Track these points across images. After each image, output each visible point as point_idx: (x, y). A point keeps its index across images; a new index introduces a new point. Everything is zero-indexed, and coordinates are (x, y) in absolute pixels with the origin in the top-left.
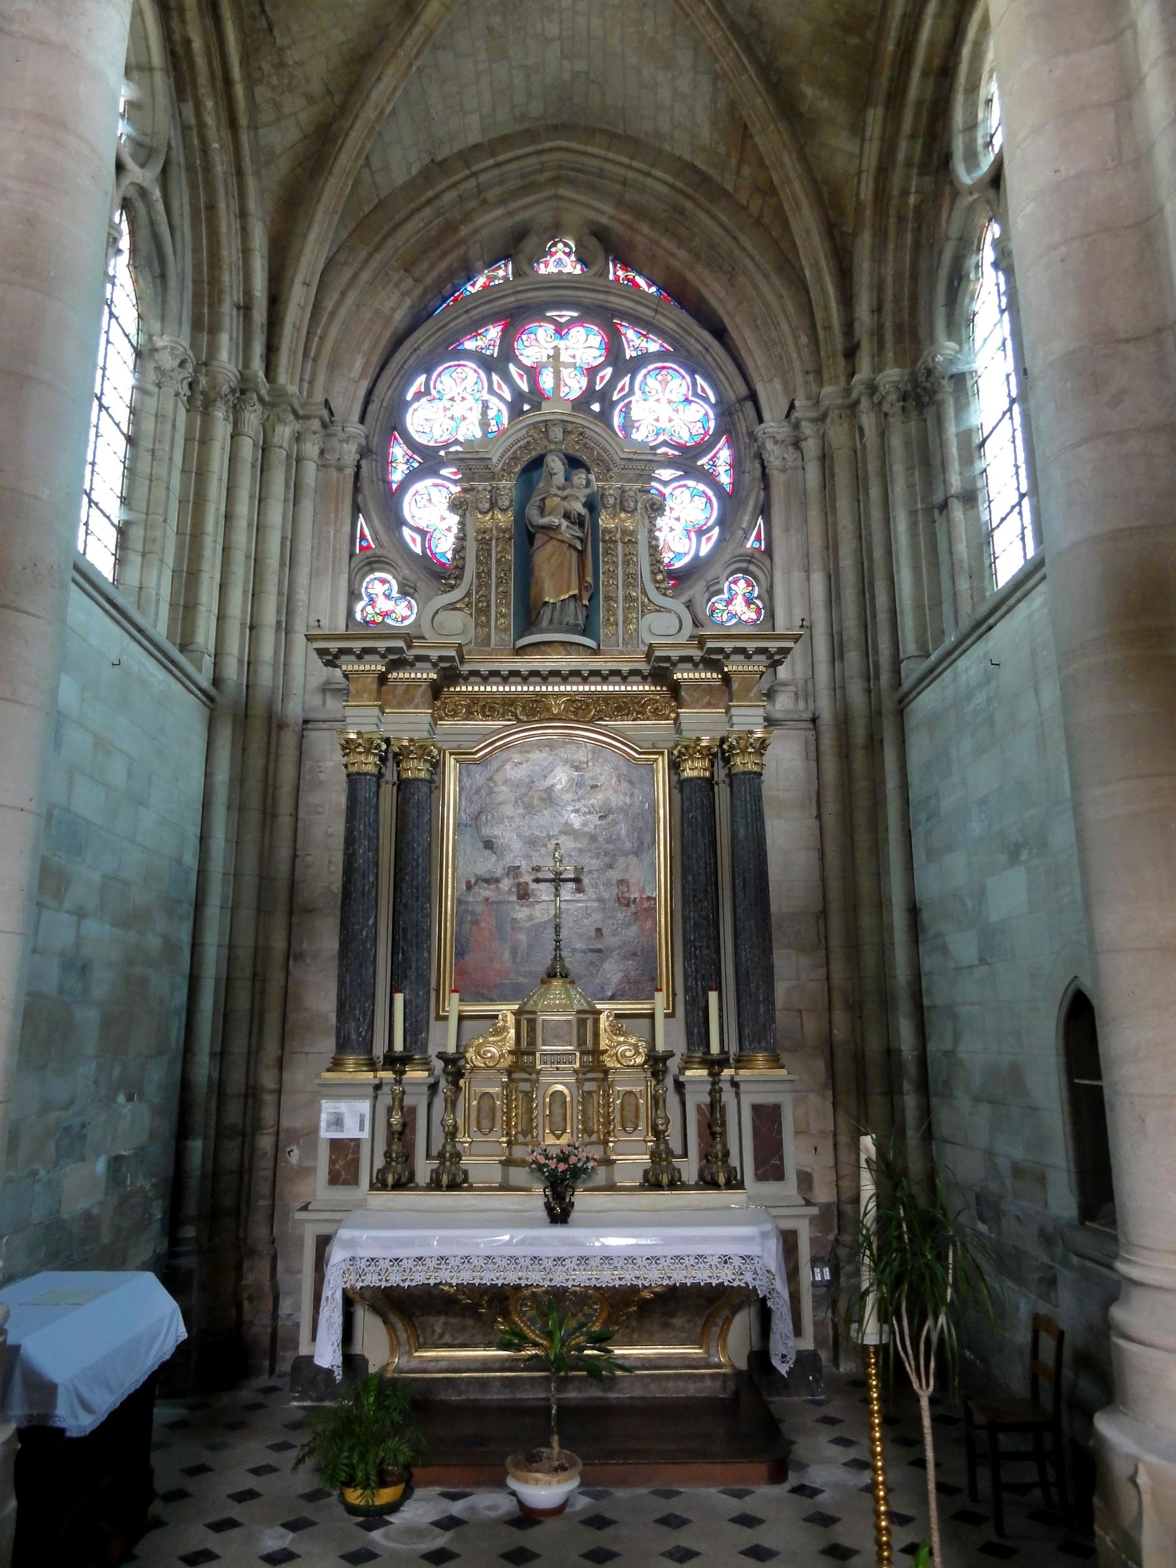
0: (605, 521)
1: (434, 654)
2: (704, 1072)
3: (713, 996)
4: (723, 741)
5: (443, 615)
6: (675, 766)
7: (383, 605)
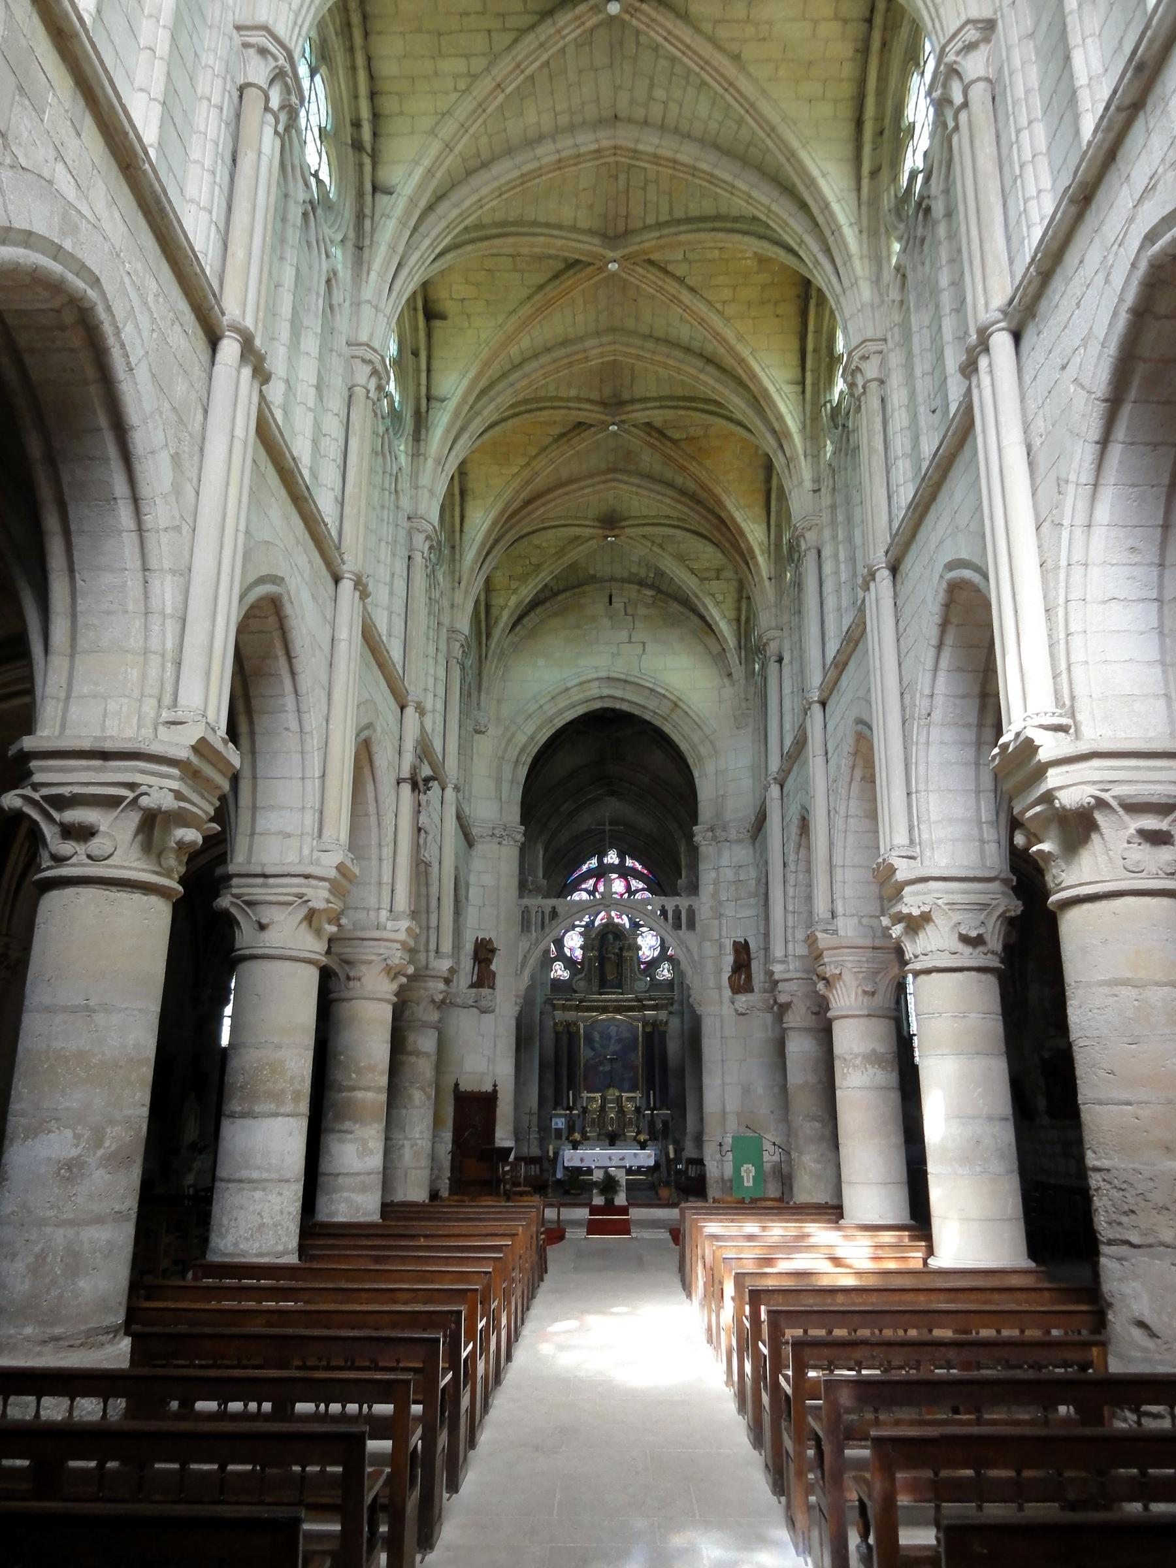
0: (625, 954)
7: (559, 972)
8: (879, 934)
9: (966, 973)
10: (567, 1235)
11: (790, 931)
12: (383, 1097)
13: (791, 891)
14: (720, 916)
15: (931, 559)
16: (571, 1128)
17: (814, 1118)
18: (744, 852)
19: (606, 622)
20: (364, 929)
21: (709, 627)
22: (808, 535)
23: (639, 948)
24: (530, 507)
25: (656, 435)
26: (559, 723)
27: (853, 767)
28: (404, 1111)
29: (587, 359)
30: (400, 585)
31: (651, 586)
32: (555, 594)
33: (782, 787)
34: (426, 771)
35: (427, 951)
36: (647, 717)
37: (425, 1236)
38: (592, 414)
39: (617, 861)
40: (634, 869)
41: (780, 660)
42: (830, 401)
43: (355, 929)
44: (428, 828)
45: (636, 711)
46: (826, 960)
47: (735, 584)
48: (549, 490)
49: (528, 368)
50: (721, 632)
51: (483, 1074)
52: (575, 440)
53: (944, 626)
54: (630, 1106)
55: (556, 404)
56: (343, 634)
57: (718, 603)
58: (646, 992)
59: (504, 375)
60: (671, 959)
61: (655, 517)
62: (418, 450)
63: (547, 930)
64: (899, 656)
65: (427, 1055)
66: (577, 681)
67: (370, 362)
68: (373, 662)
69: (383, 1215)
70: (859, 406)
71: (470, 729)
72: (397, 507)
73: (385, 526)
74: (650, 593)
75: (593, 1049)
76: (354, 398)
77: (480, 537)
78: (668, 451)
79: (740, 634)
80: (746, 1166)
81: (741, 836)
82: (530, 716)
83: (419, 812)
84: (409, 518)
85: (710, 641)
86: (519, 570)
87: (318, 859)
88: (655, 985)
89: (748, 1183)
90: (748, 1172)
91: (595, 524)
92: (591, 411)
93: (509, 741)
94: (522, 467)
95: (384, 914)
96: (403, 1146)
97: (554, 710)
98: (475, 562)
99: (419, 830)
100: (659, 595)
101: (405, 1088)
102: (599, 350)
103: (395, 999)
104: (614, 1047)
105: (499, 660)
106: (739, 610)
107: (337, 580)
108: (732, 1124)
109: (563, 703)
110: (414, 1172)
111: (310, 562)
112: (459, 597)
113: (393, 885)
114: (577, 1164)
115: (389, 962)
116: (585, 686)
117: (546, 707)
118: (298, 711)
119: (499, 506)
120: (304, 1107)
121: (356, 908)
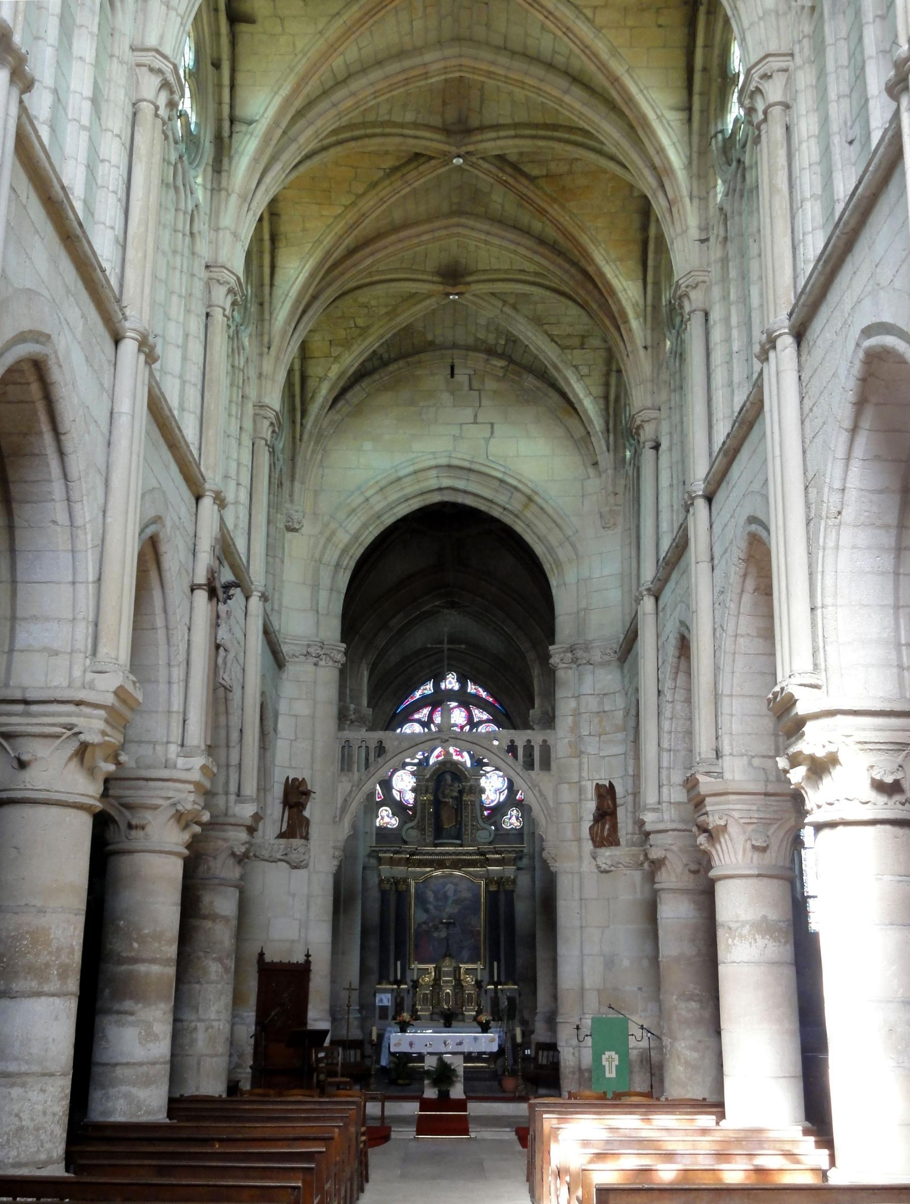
0: (465, 798)
1: (409, 850)
2: (492, 987)
3: (495, 964)
4: (502, 878)
5: (410, 830)
6: (487, 885)
7: (387, 820)
8: (772, 778)
9: (879, 826)
10: (393, 1135)
11: (664, 773)
12: (171, 971)
13: (666, 725)
14: (580, 754)
15: (845, 323)
16: (399, 1006)
17: (691, 998)
18: (610, 677)
19: (446, 397)
20: (149, 767)
21: (570, 405)
22: (693, 295)
23: (482, 791)
24: (358, 256)
25: (509, 170)
26: (389, 520)
27: (745, 576)
28: (197, 986)
29: (426, 76)
30: (195, 349)
31: (502, 356)
32: (385, 364)
33: (657, 599)
34: (227, 576)
35: (227, 793)
36: (496, 513)
37: (220, 1140)
38: (433, 143)
39: (456, 686)
40: (477, 697)
41: (657, 447)
42: (722, 131)
43: (138, 767)
44: (228, 645)
45: (483, 506)
46: (708, 808)
47: (603, 353)
48: (380, 236)
49: (354, 85)
50: (586, 411)
51: (293, 941)
52: (409, 177)
53: (860, 404)
54: (469, 980)
55: (387, 130)
56: (124, 406)
57: (581, 377)
58: (490, 843)
59: (325, 93)
60: (520, 805)
61: (506, 271)
62: (220, 183)
63: (372, 769)
64: (803, 442)
65: (226, 919)
66: (411, 469)
67: (160, 71)
68: (161, 441)
69: (170, 1114)
70: (759, 136)
71: (281, 525)
72: (193, 253)
73: (177, 273)
74: (501, 363)
75: (426, 911)
76: (139, 116)
77: (294, 293)
78: (525, 191)
79: (608, 414)
80: (608, 1053)
81: (607, 658)
82: (354, 510)
83: (218, 625)
84: (207, 267)
85: (573, 422)
86: (342, 333)
87: (92, 682)
88: (502, 835)
89: (611, 1073)
90: (611, 1062)
91: (436, 279)
92: (431, 140)
93: (329, 540)
94: (346, 207)
95: (173, 749)
96: (195, 1029)
97: (383, 504)
98: (288, 322)
99: (218, 647)
100: (512, 367)
101: (199, 958)
102: (442, 64)
103: (186, 852)
104: (451, 909)
105: (317, 442)
106: (607, 385)
107: (117, 340)
108: (592, 1002)
109: (393, 495)
110: (208, 1060)
111: (83, 316)
112: (267, 367)
113: (185, 713)
114: (405, 1049)
115: (180, 807)
116: (421, 475)
117: (372, 501)
118: (68, 500)
119: (318, 254)
120: (73, 985)
121: (140, 742)
